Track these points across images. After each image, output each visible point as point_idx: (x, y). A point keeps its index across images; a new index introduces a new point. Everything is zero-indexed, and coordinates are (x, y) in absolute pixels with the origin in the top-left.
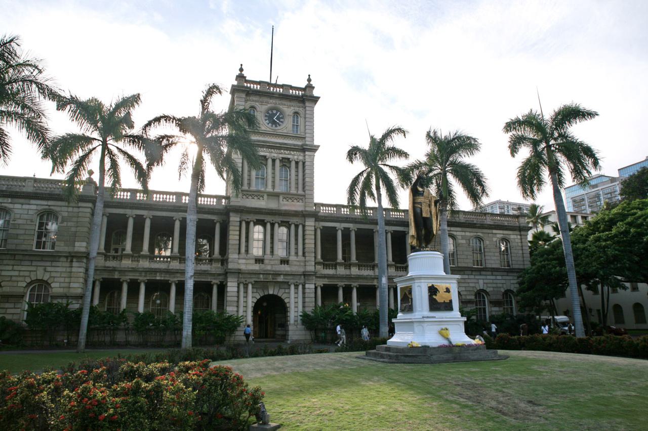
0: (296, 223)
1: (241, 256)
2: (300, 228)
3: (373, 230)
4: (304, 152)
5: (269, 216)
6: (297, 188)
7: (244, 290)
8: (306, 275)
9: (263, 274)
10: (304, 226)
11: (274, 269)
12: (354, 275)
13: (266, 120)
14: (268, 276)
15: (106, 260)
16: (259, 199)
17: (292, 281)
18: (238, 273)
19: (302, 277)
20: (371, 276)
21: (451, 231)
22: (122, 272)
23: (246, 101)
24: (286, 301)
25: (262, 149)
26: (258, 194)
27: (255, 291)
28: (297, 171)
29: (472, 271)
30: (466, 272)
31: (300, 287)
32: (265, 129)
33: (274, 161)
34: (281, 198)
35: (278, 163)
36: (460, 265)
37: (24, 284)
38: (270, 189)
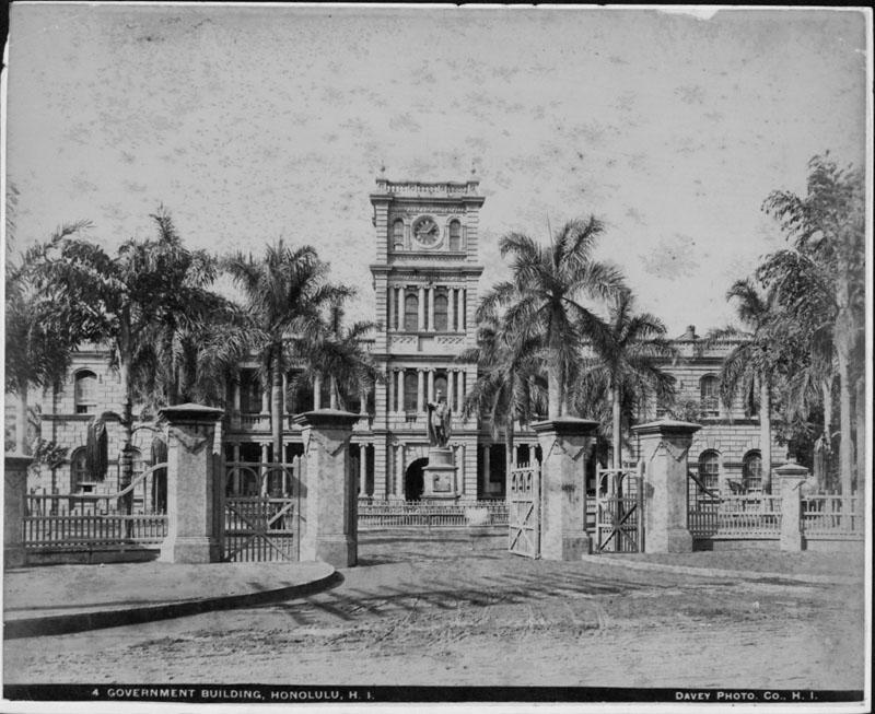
1: (392, 413)
6: (456, 324)
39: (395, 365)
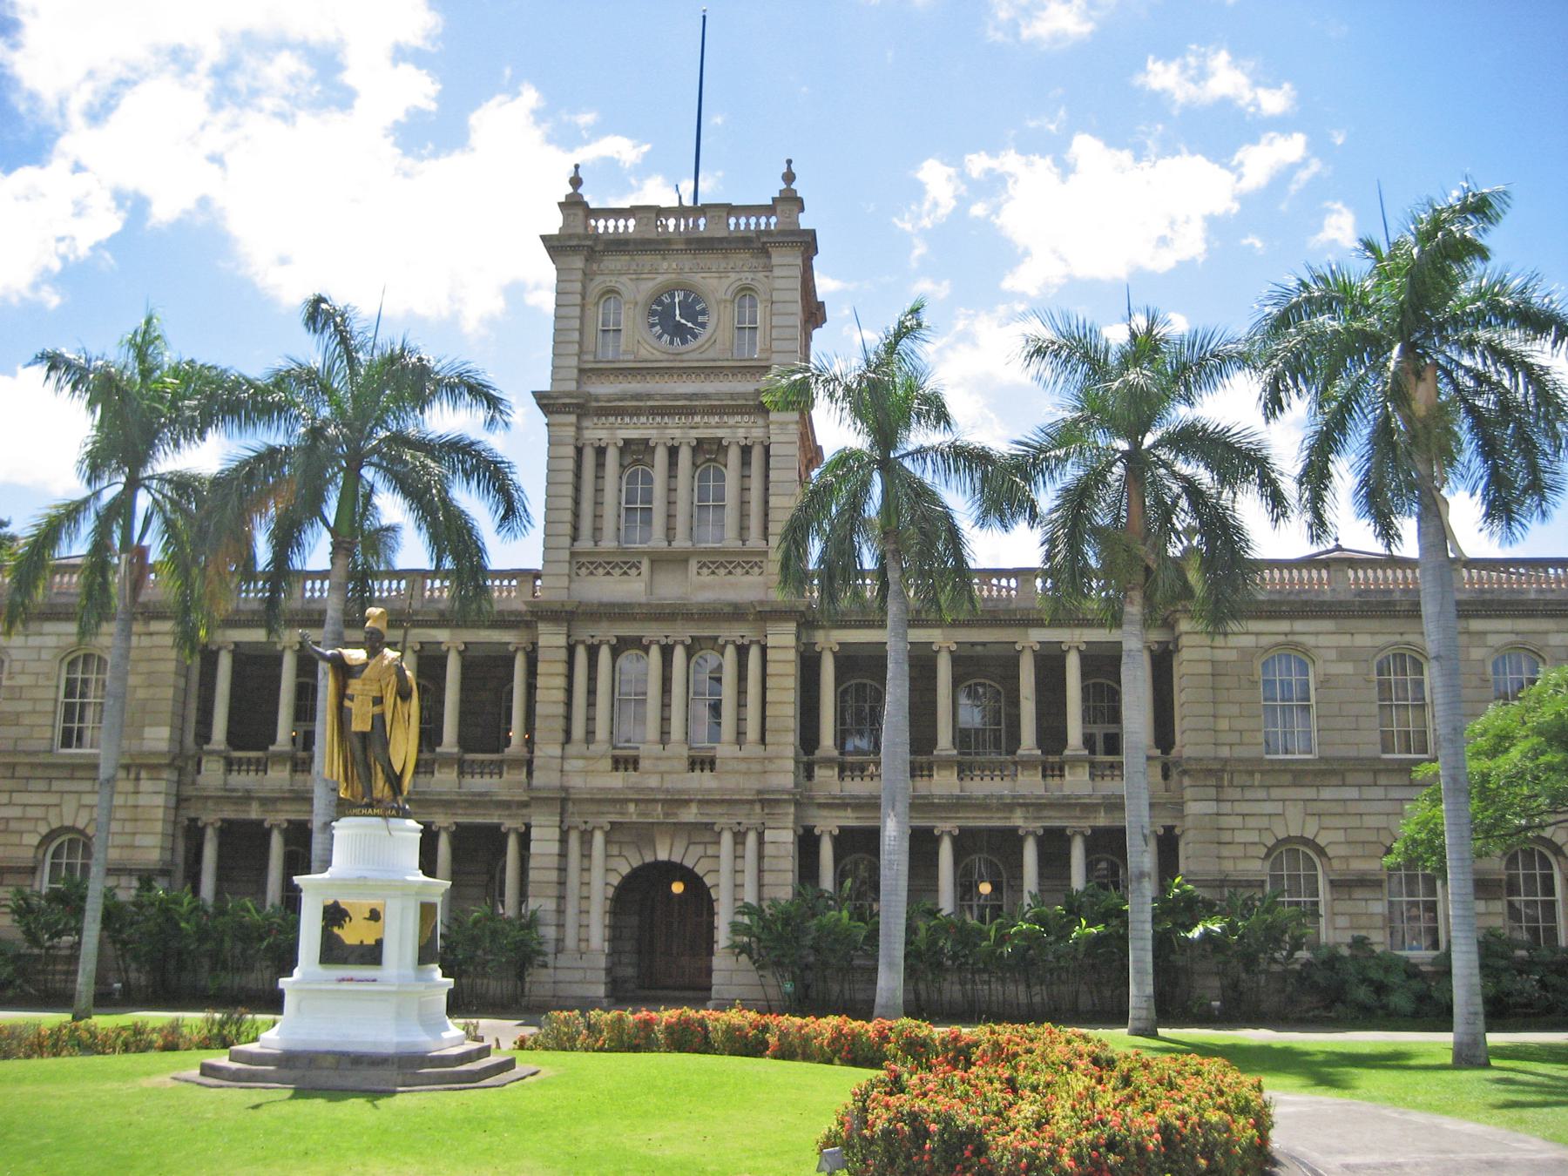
0: (739, 642)
1: (572, 749)
2: (754, 653)
5: (654, 625)
6: (743, 529)
8: (767, 801)
9: (637, 801)
10: (764, 649)
11: (667, 785)
12: (941, 797)
13: (653, 325)
14: (651, 807)
15: (229, 770)
17: (723, 820)
18: (563, 801)
19: (758, 808)
20: (1001, 797)
21: (1292, 633)
22: (266, 802)
24: (708, 881)
26: (624, 562)
27: (615, 850)
28: (744, 477)
29: (1376, 772)
30: (1350, 778)
31: (751, 839)
32: (650, 357)
33: (673, 452)
34: (693, 565)
35: (685, 456)
36: (1330, 752)
37: (35, 840)
38: (657, 541)
39: (586, 632)
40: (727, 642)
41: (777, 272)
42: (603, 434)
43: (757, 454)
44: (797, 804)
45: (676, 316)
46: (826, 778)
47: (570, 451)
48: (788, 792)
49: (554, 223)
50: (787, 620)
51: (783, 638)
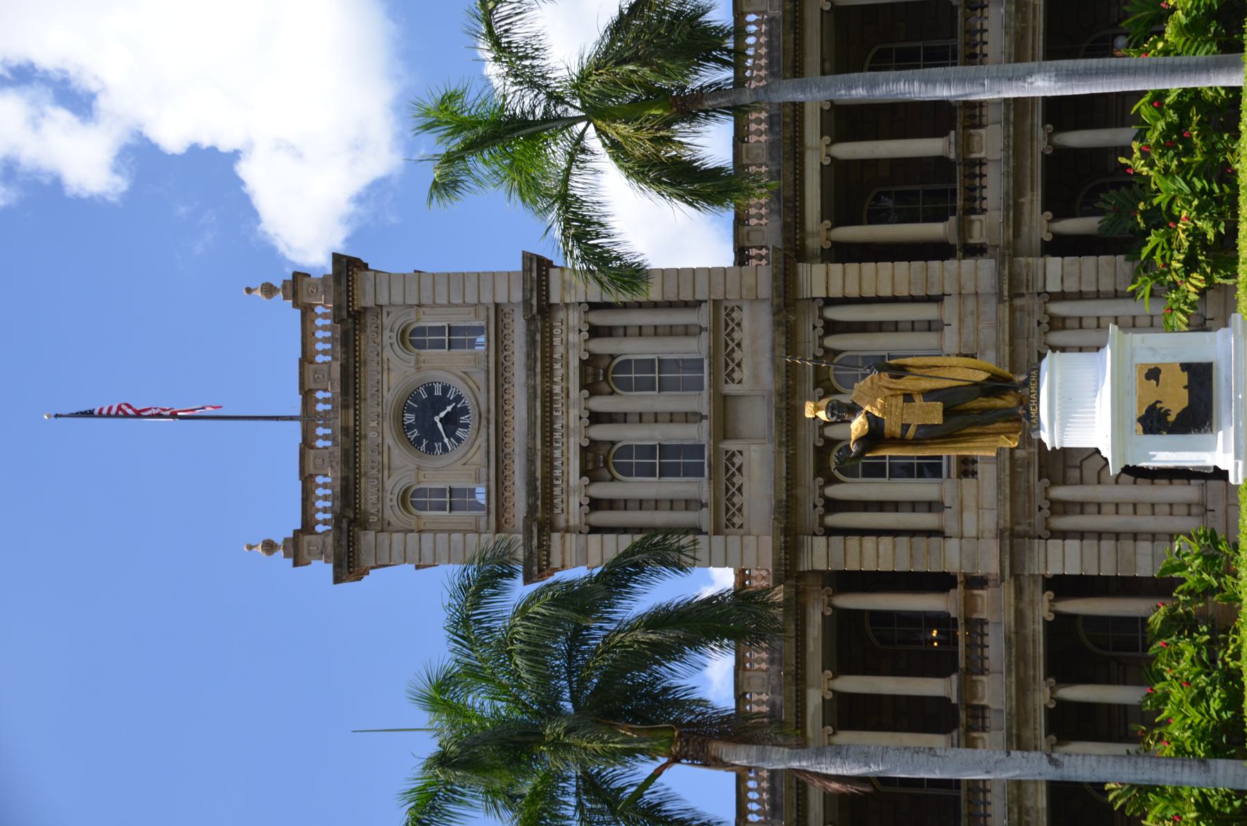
0: (820, 331)
1: (951, 527)
2: (834, 314)
3: (822, 10)
4: (551, 306)
6: (686, 331)
7: (1074, 513)
8: (1013, 289)
10: (830, 302)
16: (739, 469)
18: (1014, 538)
19: (1018, 302)
23: (384, 527)
25: (557, 463)
26: (727, 472)
27: (1075, 474)
28: (625, 331)
31: (1058, 309)
32: (483, 450)
33: (596, 418)
34: (730, 389)
35: (601, 404)
39: (810, 514)
40: (821, 346)
41: (383, 300)
42: (574, 501)
43: (599, 319)
44: (1016, 254)
45: (431, 419)
46: (986, 227)
47: (594, 539)
48: (1002, 263)
49: (322, 569)
50: (795, 274)
51: (817, 279)
